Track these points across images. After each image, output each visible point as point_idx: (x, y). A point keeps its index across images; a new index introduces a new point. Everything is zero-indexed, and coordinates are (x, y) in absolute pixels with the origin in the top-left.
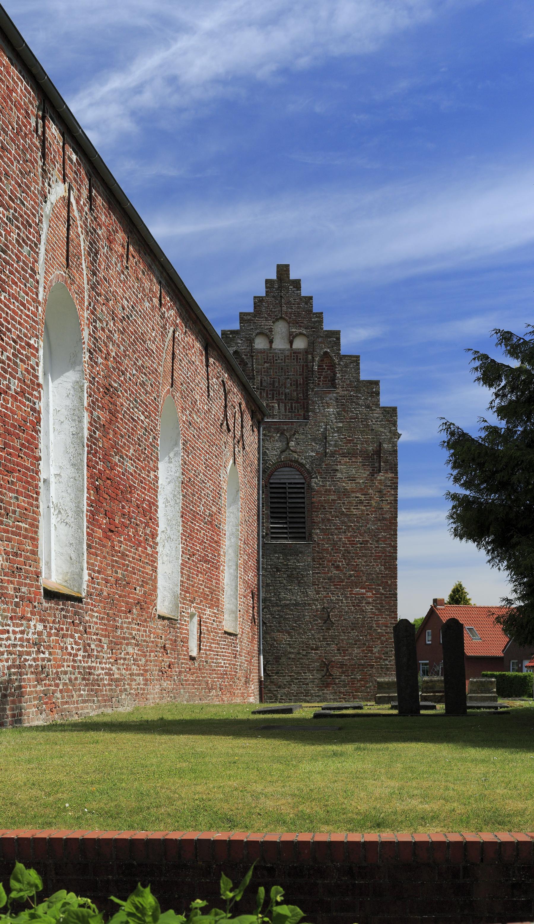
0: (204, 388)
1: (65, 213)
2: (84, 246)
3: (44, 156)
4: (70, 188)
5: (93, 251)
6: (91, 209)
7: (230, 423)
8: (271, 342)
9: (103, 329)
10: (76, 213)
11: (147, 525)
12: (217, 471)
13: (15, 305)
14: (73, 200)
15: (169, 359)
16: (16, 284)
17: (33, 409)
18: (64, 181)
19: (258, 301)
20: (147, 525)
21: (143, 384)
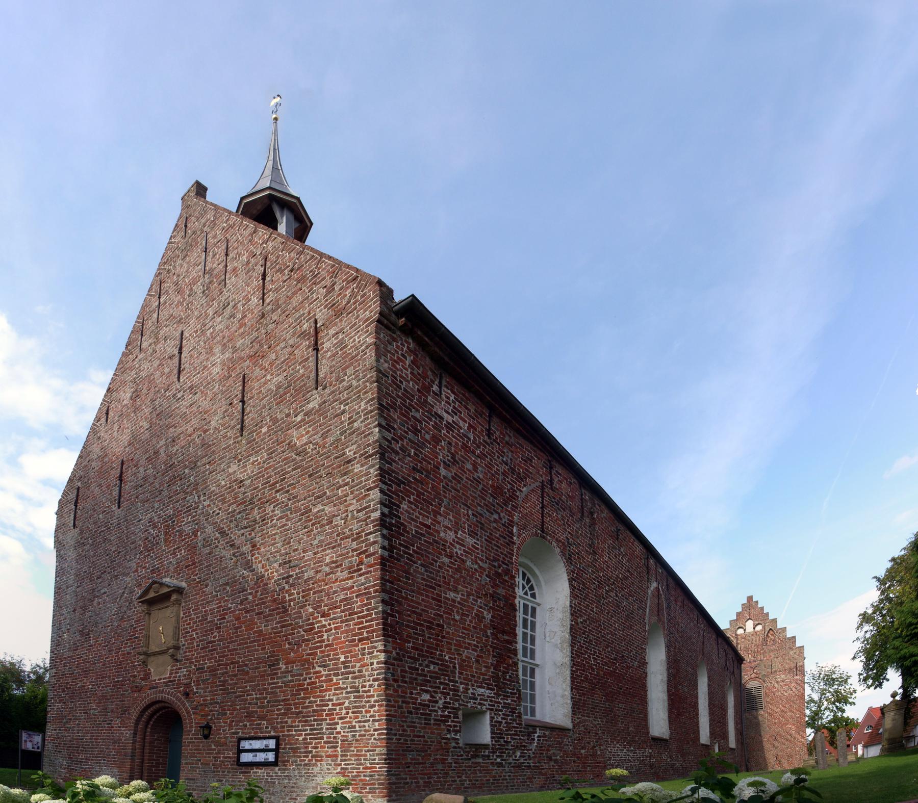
0: (717, 653)
1: (657, 593)
2: (665, 606)
3: (648, 573)
4: (659, 583)
5: (669, 607)
6: (668, 590)
7: (728, 666)
8: (745, 630)
9: (673, 637)
10: (661, 592)
11: (694, 711)
12: (723, 687)
13: (636, 633)
14: (660, 588)
15: (701, 644)
16: (636, 625)
17: (644, 672)
18: (656, 581)
19: (738, 614)
20: (694, 711)
21: (691, 656)
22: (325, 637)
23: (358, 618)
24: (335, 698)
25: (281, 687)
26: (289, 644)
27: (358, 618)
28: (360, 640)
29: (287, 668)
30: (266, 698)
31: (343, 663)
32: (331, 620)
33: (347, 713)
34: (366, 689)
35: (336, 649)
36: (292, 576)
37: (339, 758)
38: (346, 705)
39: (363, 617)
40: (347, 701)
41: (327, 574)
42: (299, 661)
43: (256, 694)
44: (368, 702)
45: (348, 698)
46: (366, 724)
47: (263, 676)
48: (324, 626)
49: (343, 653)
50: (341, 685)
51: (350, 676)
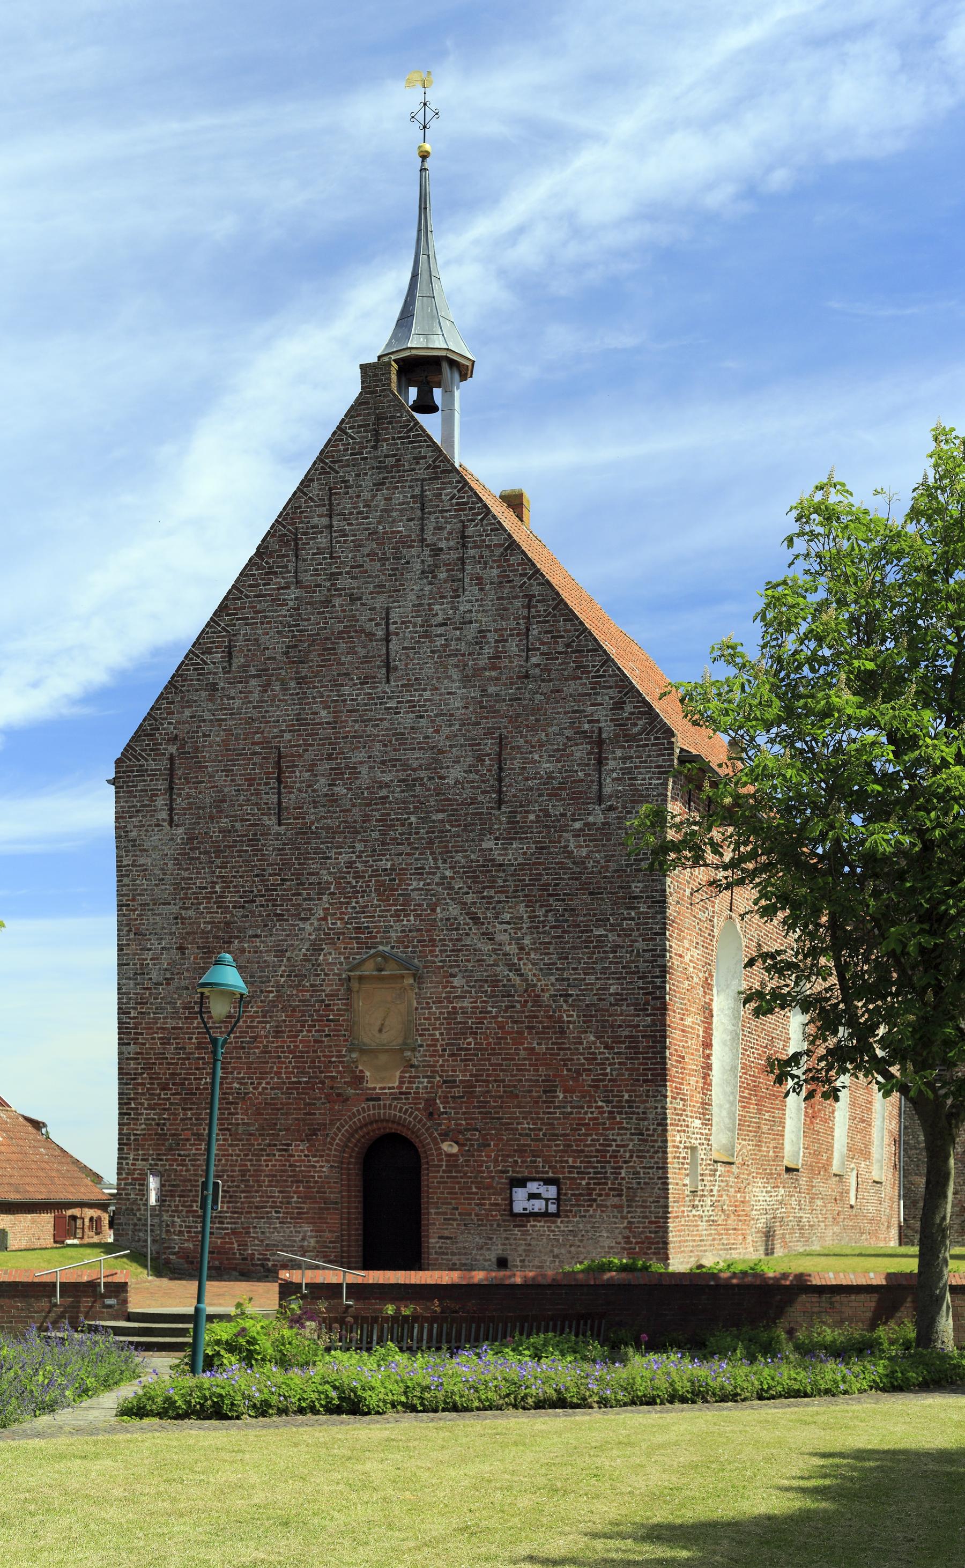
22: (608, 1070)
23: (644, 1058)
24: (619, 1138)
27: (644, 1058)
28: (645, 1081)
29: (565, 1097)
30: (540, 1130)
31: (627, 1101)
32: (615, 1053)
33: (631, 1157)
34: (651, 1132)
35: (620, 1086)
37: (625, 1210)
38: (630, 1147)
40: (631, 1144)
43: (528, 1124)
44: (653, 1146)
45: (632, 1140)
47: (537, 1102)
48: (607, 1059)
49: (627, 1091)
50: (625, 1125)
51: (635, 1116)
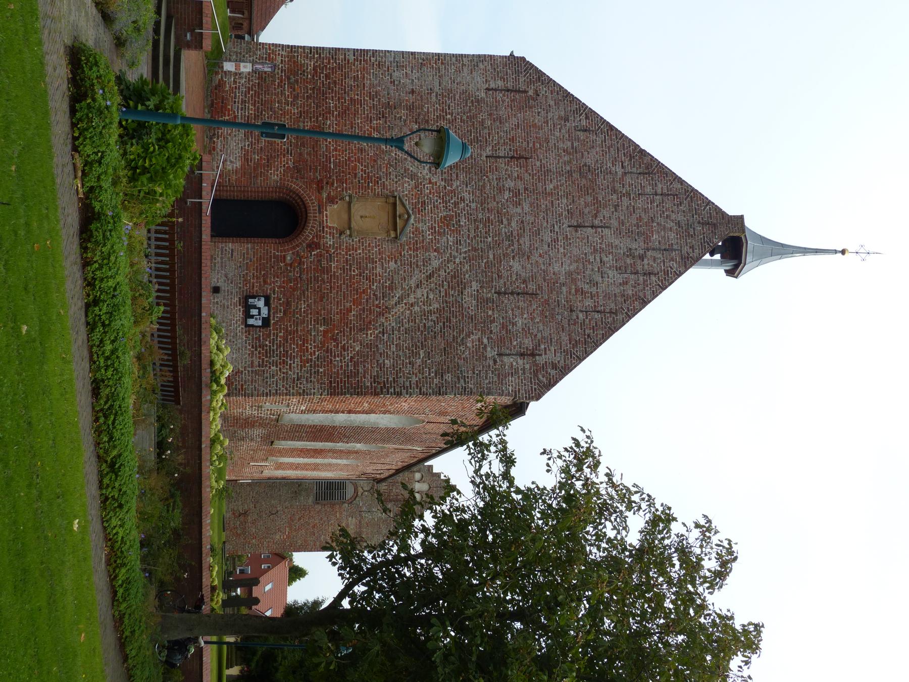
22: (337, 359)
24: (295, 365)
25: (308, 327)
26: (338, 333)
28: (331, 382)
30: (301, 316)
31: (318, 370)
33: (284, 373)
35: (328, 366)
36: (383, 336)
38: (289, 372)
39: (345, 384)
41: (378, 361)
42: (324, 341)
45: (294, 374)
46: (275, 385)
48: (344, 358)
